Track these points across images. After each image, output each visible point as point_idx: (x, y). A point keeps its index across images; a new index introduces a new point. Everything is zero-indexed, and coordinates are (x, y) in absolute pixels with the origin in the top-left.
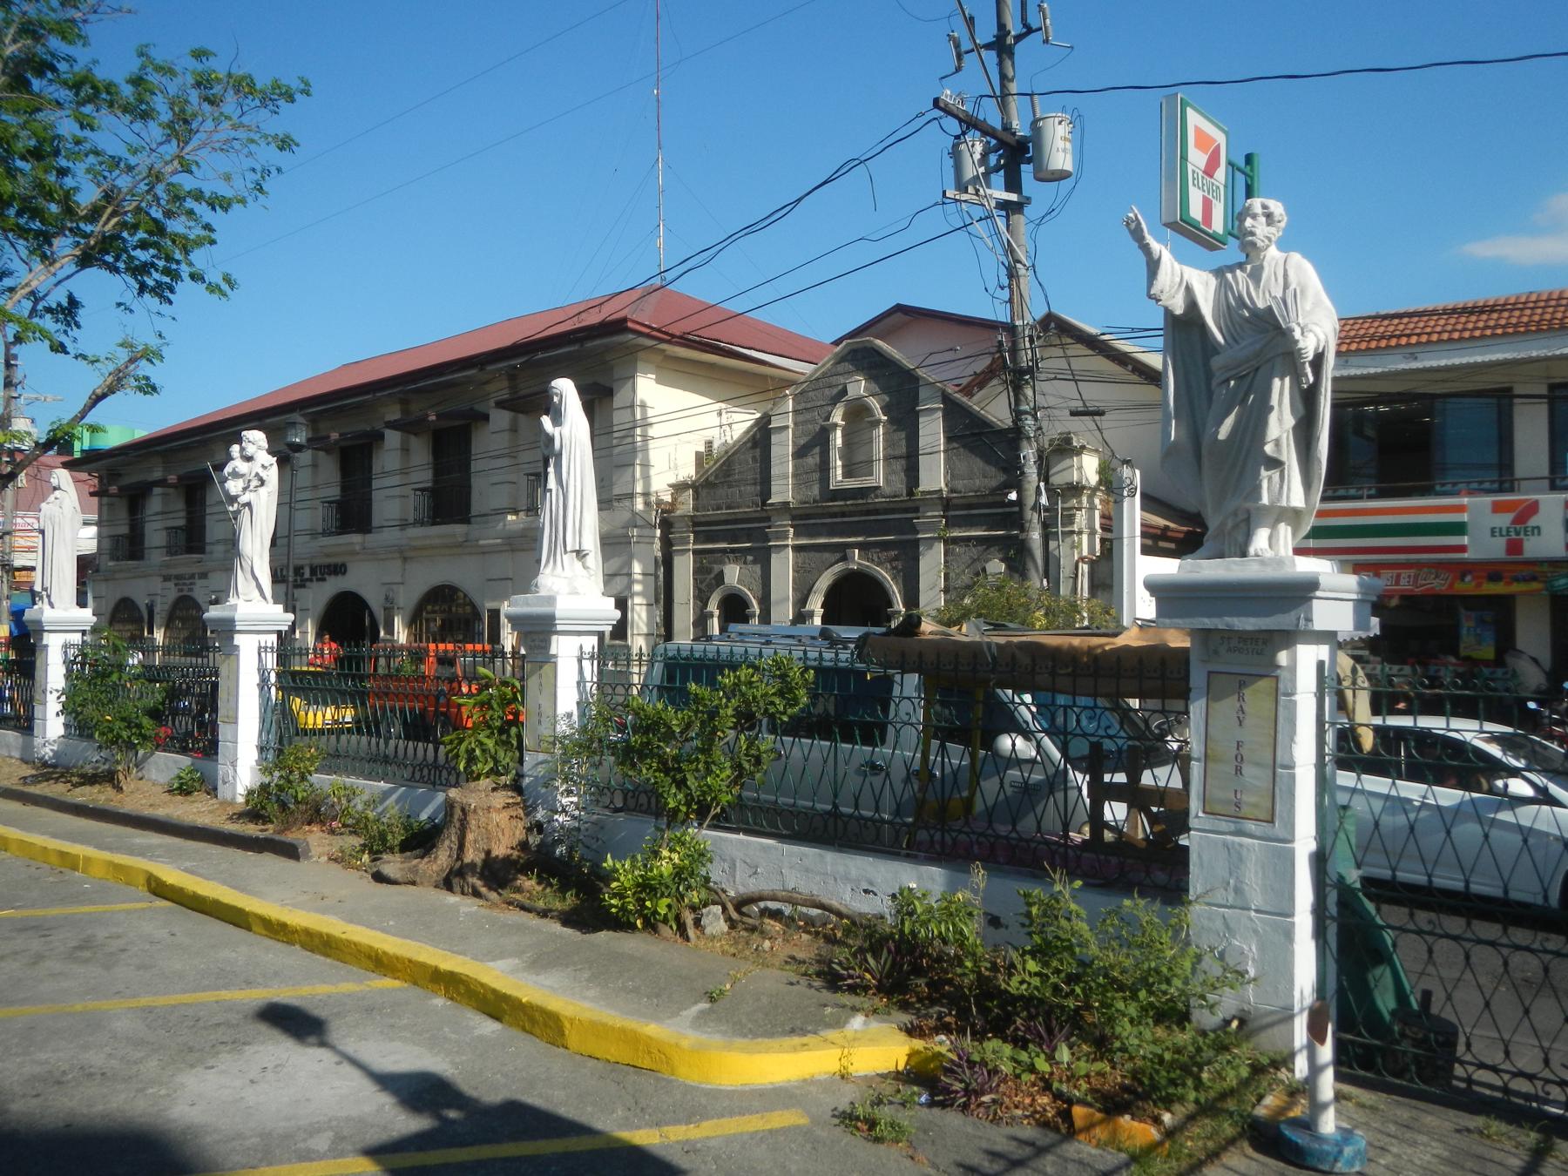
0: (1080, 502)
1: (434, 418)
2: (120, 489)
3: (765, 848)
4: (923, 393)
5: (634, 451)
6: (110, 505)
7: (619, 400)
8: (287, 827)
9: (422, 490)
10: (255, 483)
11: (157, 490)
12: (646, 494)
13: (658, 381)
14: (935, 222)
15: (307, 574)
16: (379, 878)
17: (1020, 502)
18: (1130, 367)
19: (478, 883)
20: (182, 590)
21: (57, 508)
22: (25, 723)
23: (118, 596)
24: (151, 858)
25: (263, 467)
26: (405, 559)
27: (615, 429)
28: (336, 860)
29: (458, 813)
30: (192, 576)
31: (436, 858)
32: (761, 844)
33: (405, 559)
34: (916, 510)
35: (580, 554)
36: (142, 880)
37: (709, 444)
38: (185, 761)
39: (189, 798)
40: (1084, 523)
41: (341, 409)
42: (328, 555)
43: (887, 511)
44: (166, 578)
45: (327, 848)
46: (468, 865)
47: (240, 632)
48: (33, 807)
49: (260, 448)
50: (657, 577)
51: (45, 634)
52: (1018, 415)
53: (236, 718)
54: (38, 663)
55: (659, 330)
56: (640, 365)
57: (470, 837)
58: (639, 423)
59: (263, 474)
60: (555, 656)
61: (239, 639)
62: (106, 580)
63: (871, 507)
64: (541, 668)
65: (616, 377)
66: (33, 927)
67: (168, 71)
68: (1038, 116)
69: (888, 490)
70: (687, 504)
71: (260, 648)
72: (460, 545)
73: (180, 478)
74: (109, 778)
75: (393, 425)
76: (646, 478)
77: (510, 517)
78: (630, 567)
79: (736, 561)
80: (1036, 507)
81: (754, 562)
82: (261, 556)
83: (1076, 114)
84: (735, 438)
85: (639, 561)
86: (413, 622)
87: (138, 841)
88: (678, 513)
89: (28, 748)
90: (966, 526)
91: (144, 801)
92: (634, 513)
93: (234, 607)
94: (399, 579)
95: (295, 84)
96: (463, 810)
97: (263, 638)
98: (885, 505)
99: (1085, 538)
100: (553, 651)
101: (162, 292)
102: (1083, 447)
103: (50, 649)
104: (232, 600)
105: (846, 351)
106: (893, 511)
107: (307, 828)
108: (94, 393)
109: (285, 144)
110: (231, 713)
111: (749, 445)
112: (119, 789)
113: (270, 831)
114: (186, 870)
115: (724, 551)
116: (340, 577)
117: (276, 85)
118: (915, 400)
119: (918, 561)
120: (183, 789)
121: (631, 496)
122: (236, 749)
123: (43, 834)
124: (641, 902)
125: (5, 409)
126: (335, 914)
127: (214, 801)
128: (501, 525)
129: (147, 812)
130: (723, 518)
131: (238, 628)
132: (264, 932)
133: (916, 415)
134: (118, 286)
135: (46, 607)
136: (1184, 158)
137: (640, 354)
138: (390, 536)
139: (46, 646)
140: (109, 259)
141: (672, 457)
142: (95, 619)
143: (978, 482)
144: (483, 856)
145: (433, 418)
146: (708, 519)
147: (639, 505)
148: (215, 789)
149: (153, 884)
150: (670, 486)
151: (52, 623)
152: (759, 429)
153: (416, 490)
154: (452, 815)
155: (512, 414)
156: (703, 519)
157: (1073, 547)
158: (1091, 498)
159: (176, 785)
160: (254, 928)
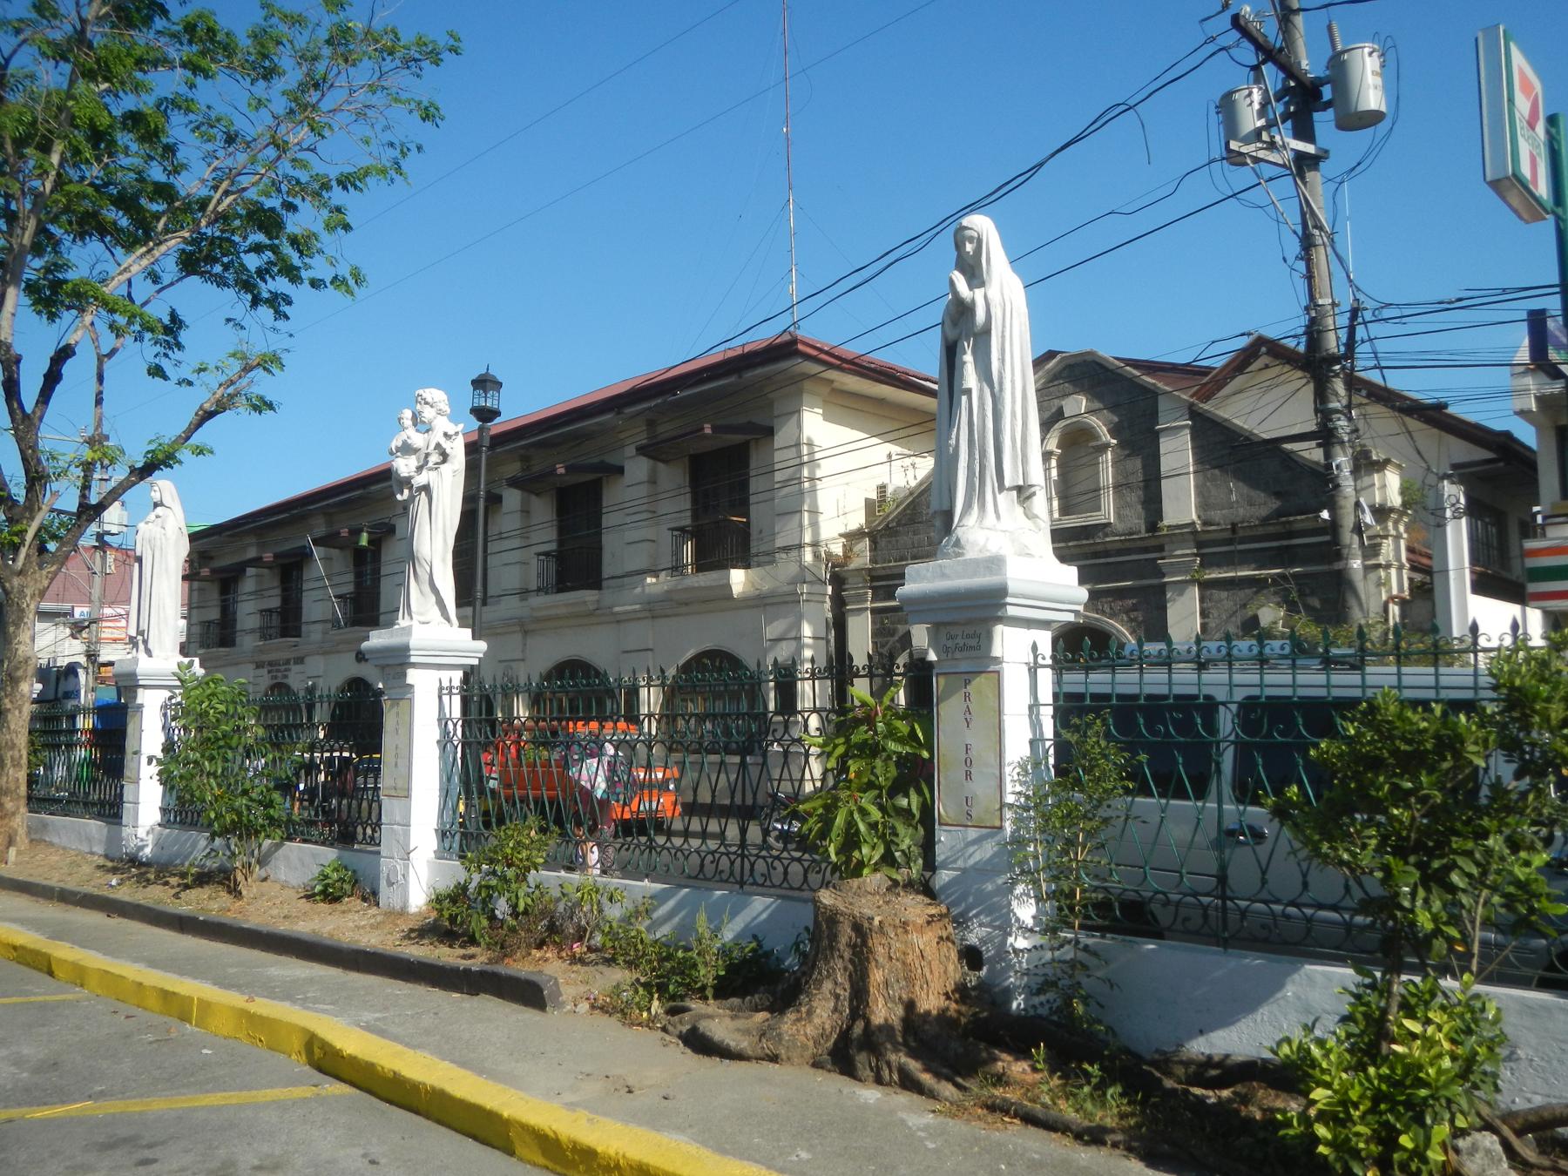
0: (1386, 528)
1: (561, 471)
2: (213, 571)
3: (1528, 1009)
4: (1163, 405)
5: (801, 493)
6: (200, 590)
7: (780, 439)
8: (504, 949)
9: (547, 554)
10: (435, 458)
11: (251, 571)
12: (815, 544)
13: (826, 418)
14: (1200, 189)
16: (699, 1043)
17: (1334, 527)
18: (1364, 393)
19: (914, 1065)
20: (276, 677)
21: (159, 529)
22: (112, 810)
24: (305, 1003)
25: (446, 435)
26: (526, 633)
28: (602, 1008)
29: (846, 934)
30: (287, 662)
31: (810, 1013)
32: (1522, 1001)
33: (526, 633)
34: (1161, 548)
35: (1023, 493)
36: (297, 1043)
37: (882, 489)
38: (329, 854)
39: (337, 906)
40: (1391, 555)
43: (1120, 552)
44: (259, 665)
45: (583, 989)
46: (880, 1028)
47: (414, 665)
48: (120, 920)
49: (440, 412)
50: (828, 642)
51: (140, 691)
52: (1324, 413)
53: (409, 789)
54: (130, 729)
55: (827, 353)
56: (806, 398)
57: (877, 976)
58: (806, 459)
59: (446, 445)
60: (998, 661)
61: (413, 676)
63: (1100, 548)
64: (967, 683)
65: (776, 413)
66: (125, 1141)
67: (296, 21)
68: (1339, 48)
69: (1120, 527)
70: (863, 556)
71: (441, 689)
72: (590, 614)
73: (276, 556)
74: (222, 878)
75: (514, 483)
76: (815, 525)
77: (649, 580)
78: (799, 629)
80: (1358, 529)
82: (444, 560)
83: (1389, 43)
84: (920, 478)
85: (810, 622)
86: (536, 701)
87: (274, 971)
88: (852, 566)
89: (114, 840)
90: (1228, 565)
91: (275, 912)
92: (803, 568)
93: (408, 631)
94: (520, 657)
95: (443, 41)
96: (857, 928)
97: (445, 675)
98: (1119, 546)
99: (1393, 572)
100: (996, 651)
101: (277, 303)
102: (1387, 462)
103: (145, 711)
104: (403, 622)
105: (1060, 367)
106: (1128, 551)
107: (537, 954)
108: (201, 408)
109: (428, 114)
110: (400, 783)
112: (235, 892)
113: (479, 959)
114: (368, 1028)
117: (421, 43)
118: (1154, 416)
119: (1164, 609)
120: (328, 894)
121: (800, 546)
122: (407, 835)
123: (136, 960)
124: (1387, 1138)
125: (96, 429)
126: (679, 1129)
127: (374, 910)
128: (639, 590)
129: (283, 927)
131: (413, 659)
132: (541, 1160)
133: (1155, 437)
134: (230, 301)
135: (142, 655)
136: (1511, 100)
137: (807, 385)
138: (510, 607)
139: (141, 706)
140: (218, 269)
141: (841, 506)
143: (1241, 511)
144: (900, 1011)
145: (561, 471)
146: (889, 572)
147: (808, 556)
148: (375, 893)
149: (317, 1052)
150: (841, 535)
151: (149, 676)
153: (539, 554)
154: (833, 937)
155: (651, 462)
156: (883, 573)
157: (1379, 584)
158: (1396, 523)
159: (318, 888)
160: (519, 1150)
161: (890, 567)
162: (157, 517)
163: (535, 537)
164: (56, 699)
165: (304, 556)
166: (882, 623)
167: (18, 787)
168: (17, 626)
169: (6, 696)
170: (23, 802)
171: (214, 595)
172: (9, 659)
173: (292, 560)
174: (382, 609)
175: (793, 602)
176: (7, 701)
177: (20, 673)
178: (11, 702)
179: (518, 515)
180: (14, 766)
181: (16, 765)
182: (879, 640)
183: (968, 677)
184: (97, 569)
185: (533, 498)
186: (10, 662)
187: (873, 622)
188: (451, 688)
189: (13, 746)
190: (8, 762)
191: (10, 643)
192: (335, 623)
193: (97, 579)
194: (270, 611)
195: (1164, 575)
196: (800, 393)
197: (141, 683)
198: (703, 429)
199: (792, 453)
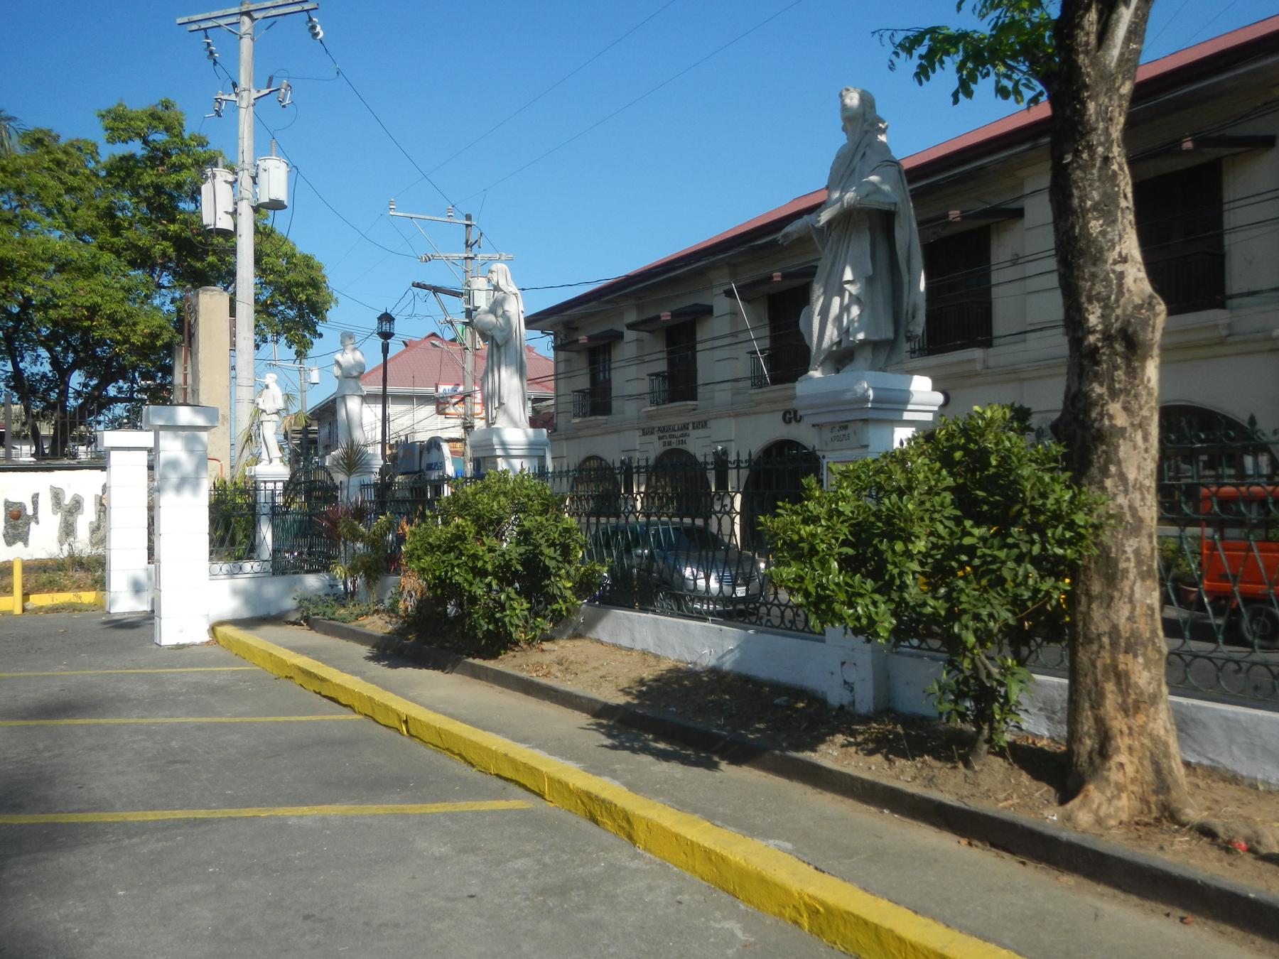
2: (590, 338)
6: (567, 361)
20: (670, 443)
23: (583, 456)
30: (685, 427)
44: (646, 432)
62: (567, 439)
72: (1222, 342)
164: (421, 471)
165: (708, 311)
169: (1114, 395)
171: (582, 364)
173: (689, 318)
174: (700, 381)
176: (1115, 408)
178: (1126, 408)
184: (468, 345)
186: (1106, 307)
188: (738, 461)
189: (1137, 528)
191: (1098, 259)
192: (758, 381)
193: (469, 355)
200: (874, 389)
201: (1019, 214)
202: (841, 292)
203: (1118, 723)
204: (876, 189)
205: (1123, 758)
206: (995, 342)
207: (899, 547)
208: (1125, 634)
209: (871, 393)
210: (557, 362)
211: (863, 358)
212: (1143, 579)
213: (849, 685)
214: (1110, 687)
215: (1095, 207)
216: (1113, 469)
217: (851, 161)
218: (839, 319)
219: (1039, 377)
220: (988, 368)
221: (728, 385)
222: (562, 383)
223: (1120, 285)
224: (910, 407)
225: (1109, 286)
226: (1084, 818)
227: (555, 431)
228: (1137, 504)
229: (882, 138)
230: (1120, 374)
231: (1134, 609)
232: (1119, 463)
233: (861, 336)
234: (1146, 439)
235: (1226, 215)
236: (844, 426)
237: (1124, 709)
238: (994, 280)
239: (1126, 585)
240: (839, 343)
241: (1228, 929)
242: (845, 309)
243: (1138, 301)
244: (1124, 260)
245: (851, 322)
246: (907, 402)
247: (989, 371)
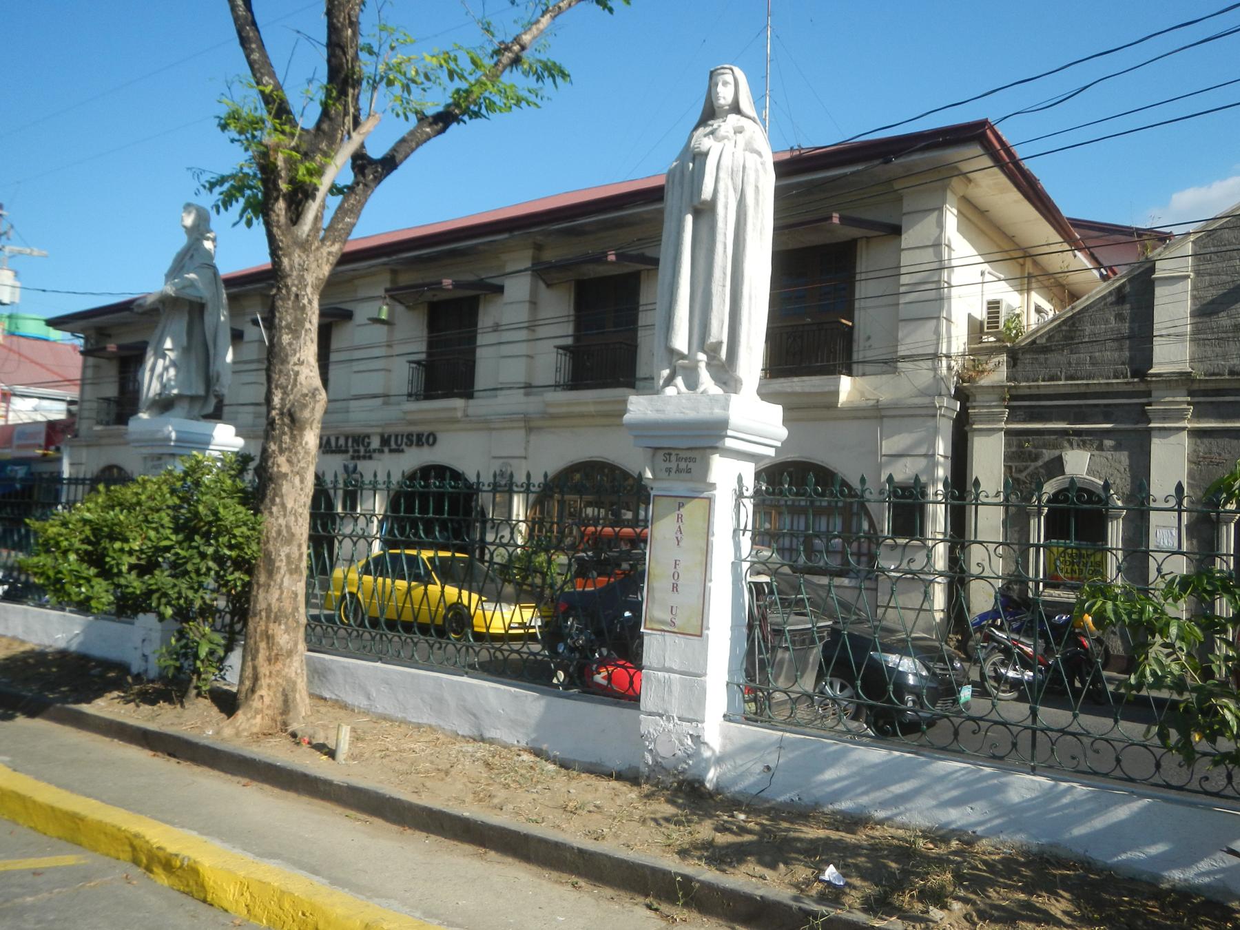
2: (120, 347)
6: (96, 367)
15: (375, 443)
26: (530, 430)
27: (903, 270)
33: (530, 430)
41: (453, 253)
42: (411, 423)
62: (88, 446)
65: (904, 211)
70: (997, 373)
78: (933, 445)
79: (1083, 445)
81: (1117, 448)
88: (985, 381)
94: (522, 453)
111: (1111, 299)
115: (1064, 432)
116: (426, 449)
121: (936, 356)
130: (1063, 391)
138: (513, 401)
142: (783, 433)
152: (1130, 281)
156: (1027, 392)
161: (1038, 387)
162: (739, 131)
163: (542, 332)
166: (1020, 446)
167: (296, 609)
168: (296, 335)
169: (281, 451)
170: (301, 633)
171: (111, 371)
172: (284, 388)
175: (927, 416)
176: (282, 460)
177: (306, 414)
178: (289, 461)
179: (527, 305)
180: (291, 572)
181: (294, 571)
182: (1013, 465)
183: (681, 501)
185: (542, 285)
186: (285, 393)
187: (1008, 445)
190: (282, 564)
191: (284, 361)
194: (108, 400)
195: (1150, 423)
196: (944, 189)
197: (729, 443)
198: (831, 218)
199: (928, 255)
200: (177, 432)
201: (500, 289)
202: (164, 356)
203: (264, 669)
204: (192, 284)
205: (263, 692)
206: (476, 394)
207: (117, 545)
208: (275, 609)
209: (173, 435)
210: (85, 367)
211: (181, 409)
212: (291, 574)
213: (145, 657)
214: (263, 645)
215: (288, 326)
216: (278, 500)
217: (183, 259)
218: (161, 376)
219: (504, 429)
220: (467, 416)
221: (251, 409)
222: (88, 388)
223: (295, 380)
224: (211, 447)
225: (288, 379)
226: (228, 731)
227: (76, 436)
228: (292, 524)
229: (208, 245)
230: (286, 438)
231: (282, 593)
232: (282, 496)
233: (175, 391)
234: (302, 482)
235: (641, 315)
236: (159, 457)
237: (269, 660)
238: (479, 343)
239: (278, 578)
240: (160, 394)
241: (267, 787)
242: (166, 369)
243: (305, 391)
244: (300, 363)
245: (169, 380)
246: (208, 443)
247: (468, 419)
